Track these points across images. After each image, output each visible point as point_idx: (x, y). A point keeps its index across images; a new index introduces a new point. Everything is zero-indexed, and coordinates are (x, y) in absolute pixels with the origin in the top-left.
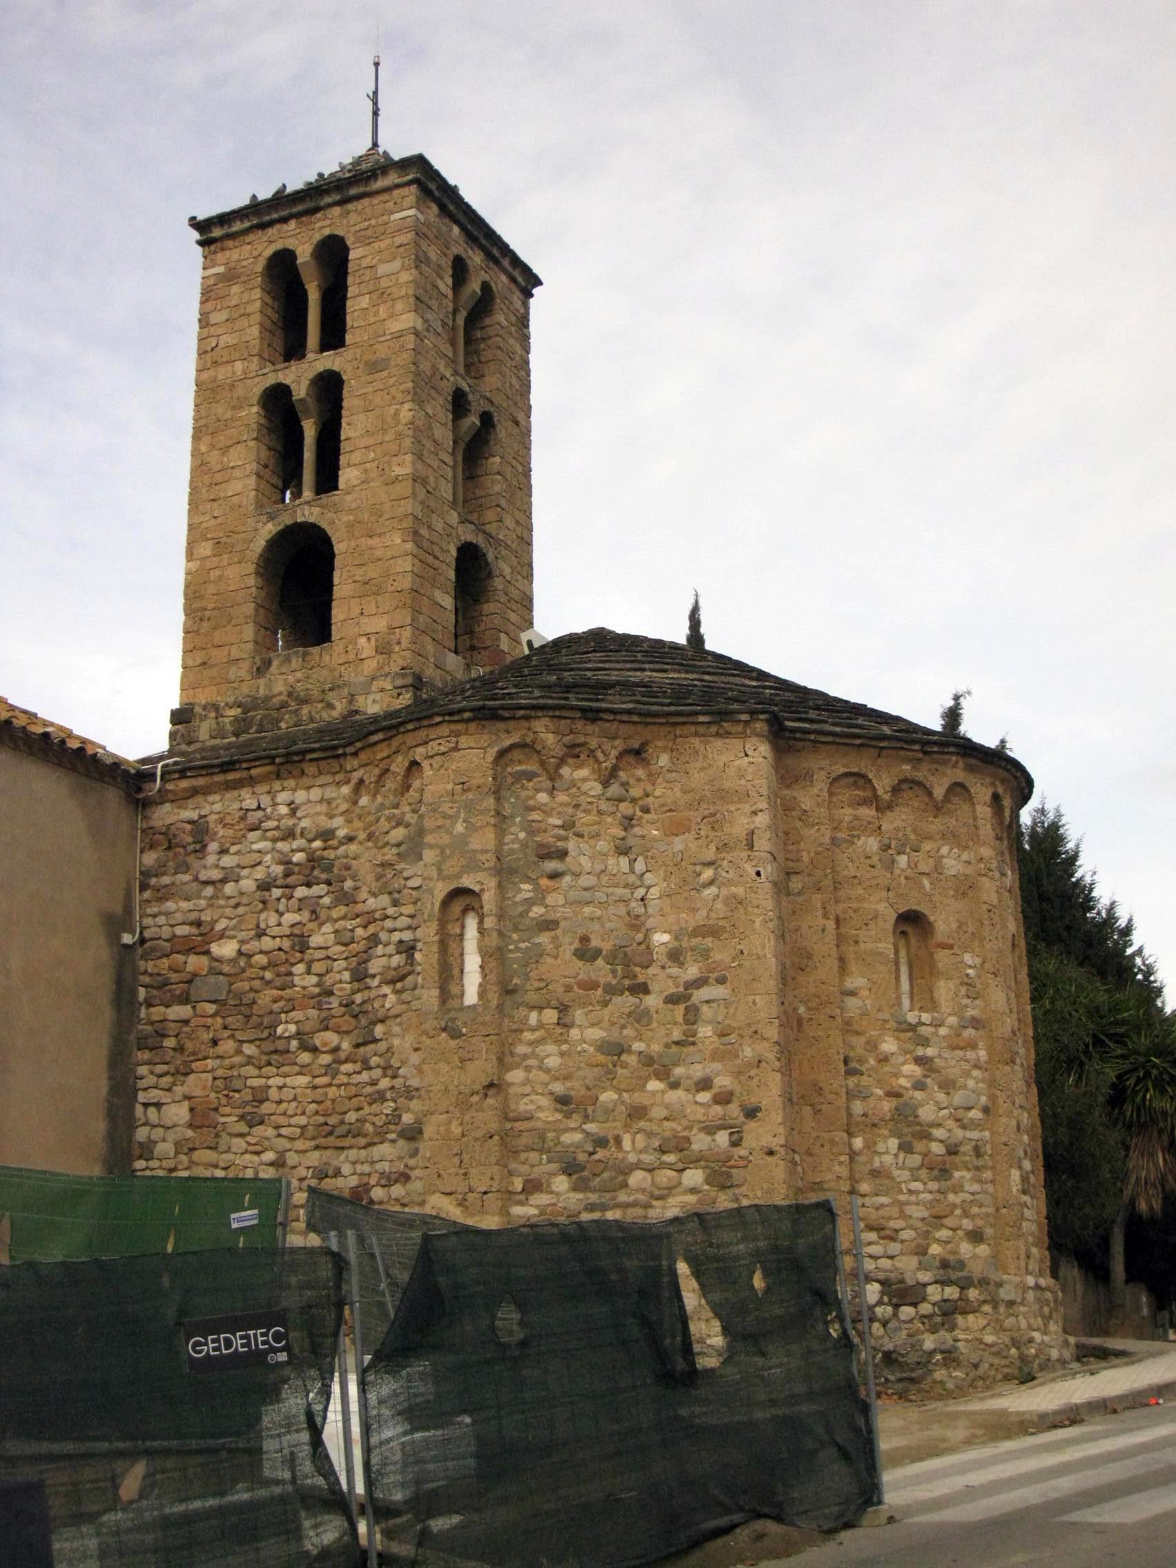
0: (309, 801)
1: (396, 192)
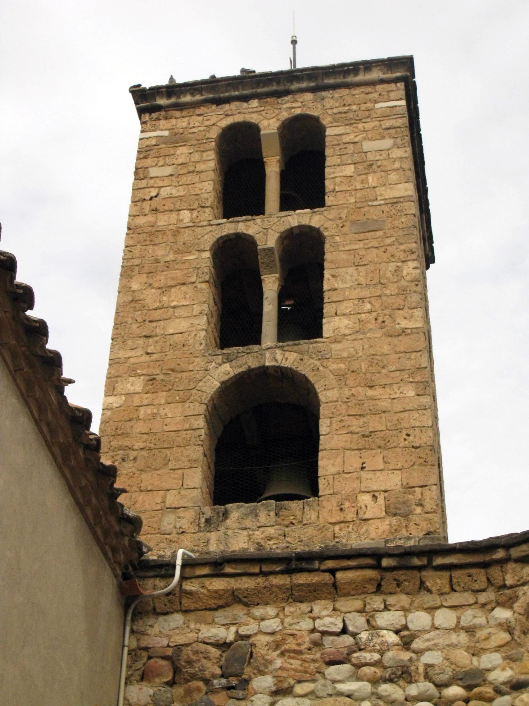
0: (435, 628)
1: (379, 87)
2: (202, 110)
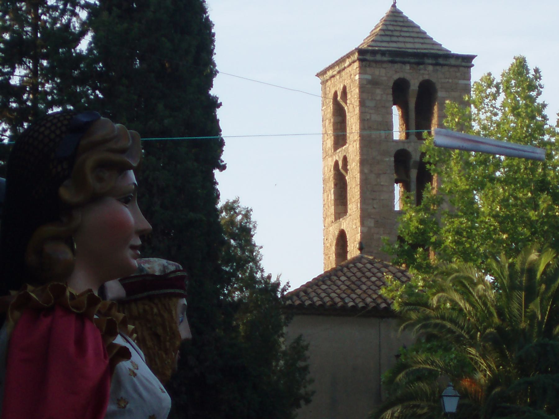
1: (461, 69)
2: (385, 65)
